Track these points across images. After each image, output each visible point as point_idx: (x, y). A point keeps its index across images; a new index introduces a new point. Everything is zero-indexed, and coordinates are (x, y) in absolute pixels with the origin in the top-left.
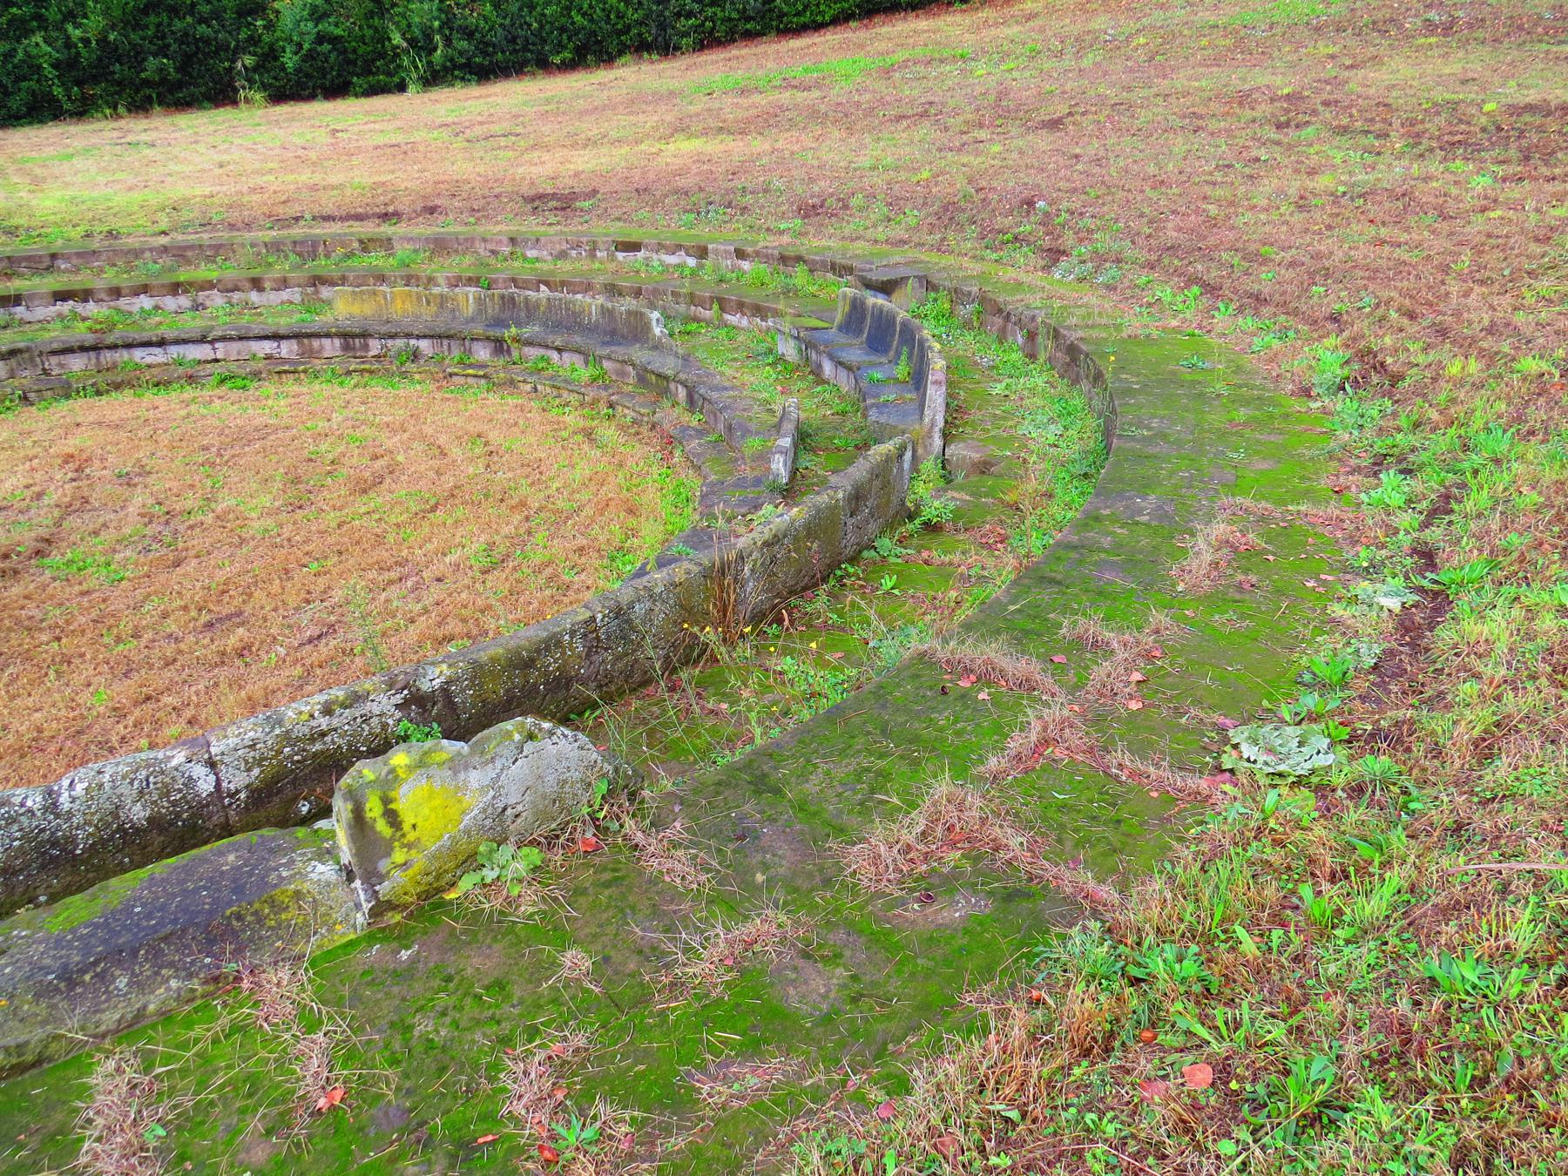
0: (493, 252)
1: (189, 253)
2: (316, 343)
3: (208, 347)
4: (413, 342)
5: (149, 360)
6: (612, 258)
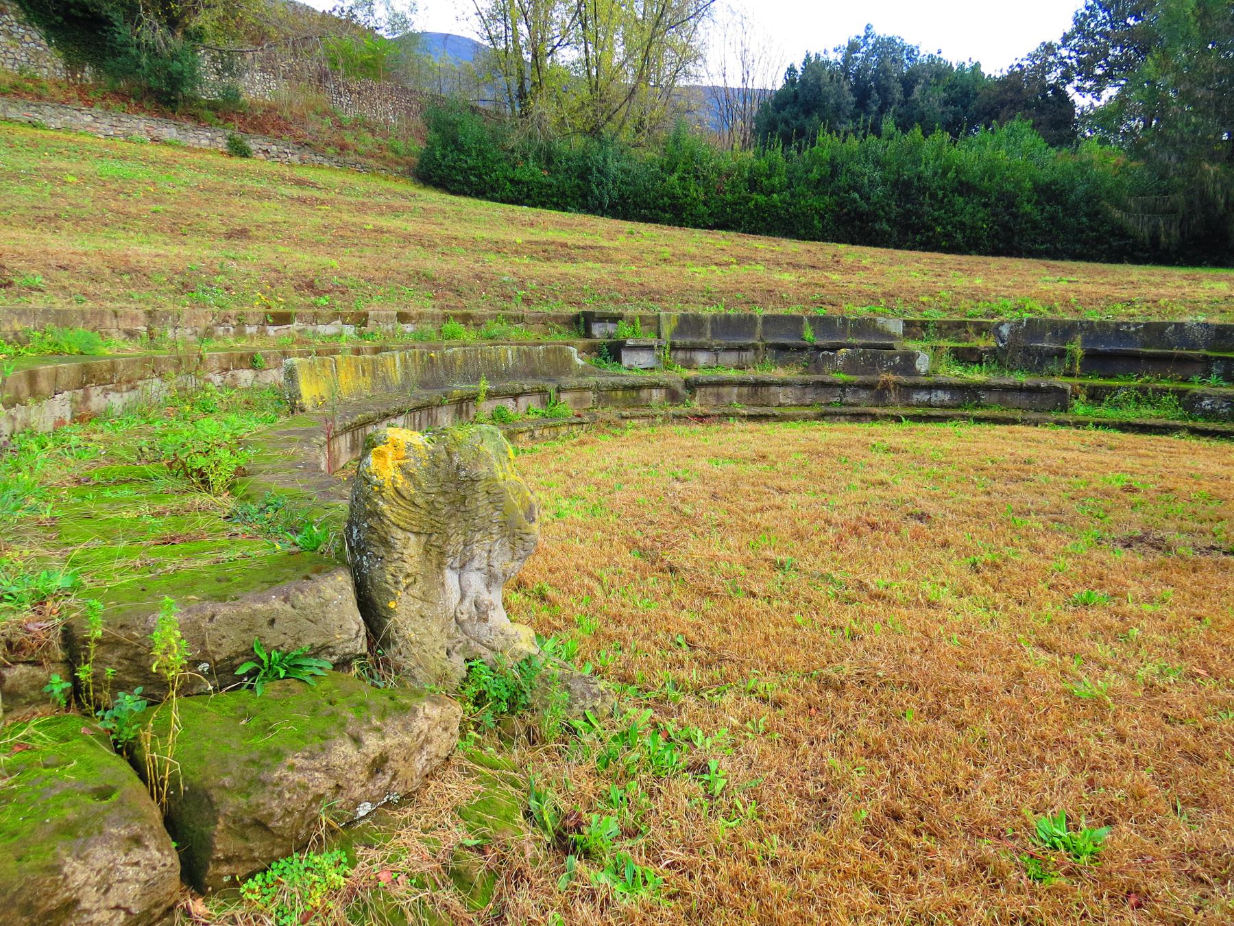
6: (262, 332)
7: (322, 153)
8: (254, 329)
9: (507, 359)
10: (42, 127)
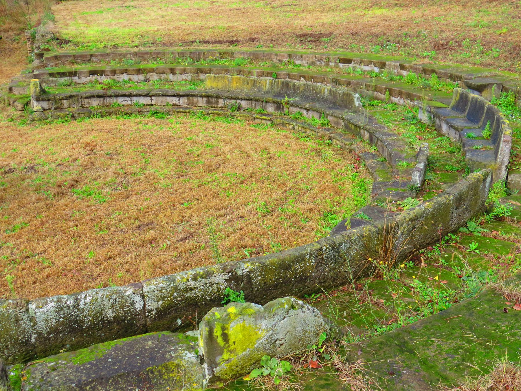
0: (280, 61)
1: (146, 56)
2: (195, 99)
3: (149, 98)
4: (239, 101)
5: (124, 103)
6: (337, 66)
9: (324, 93)
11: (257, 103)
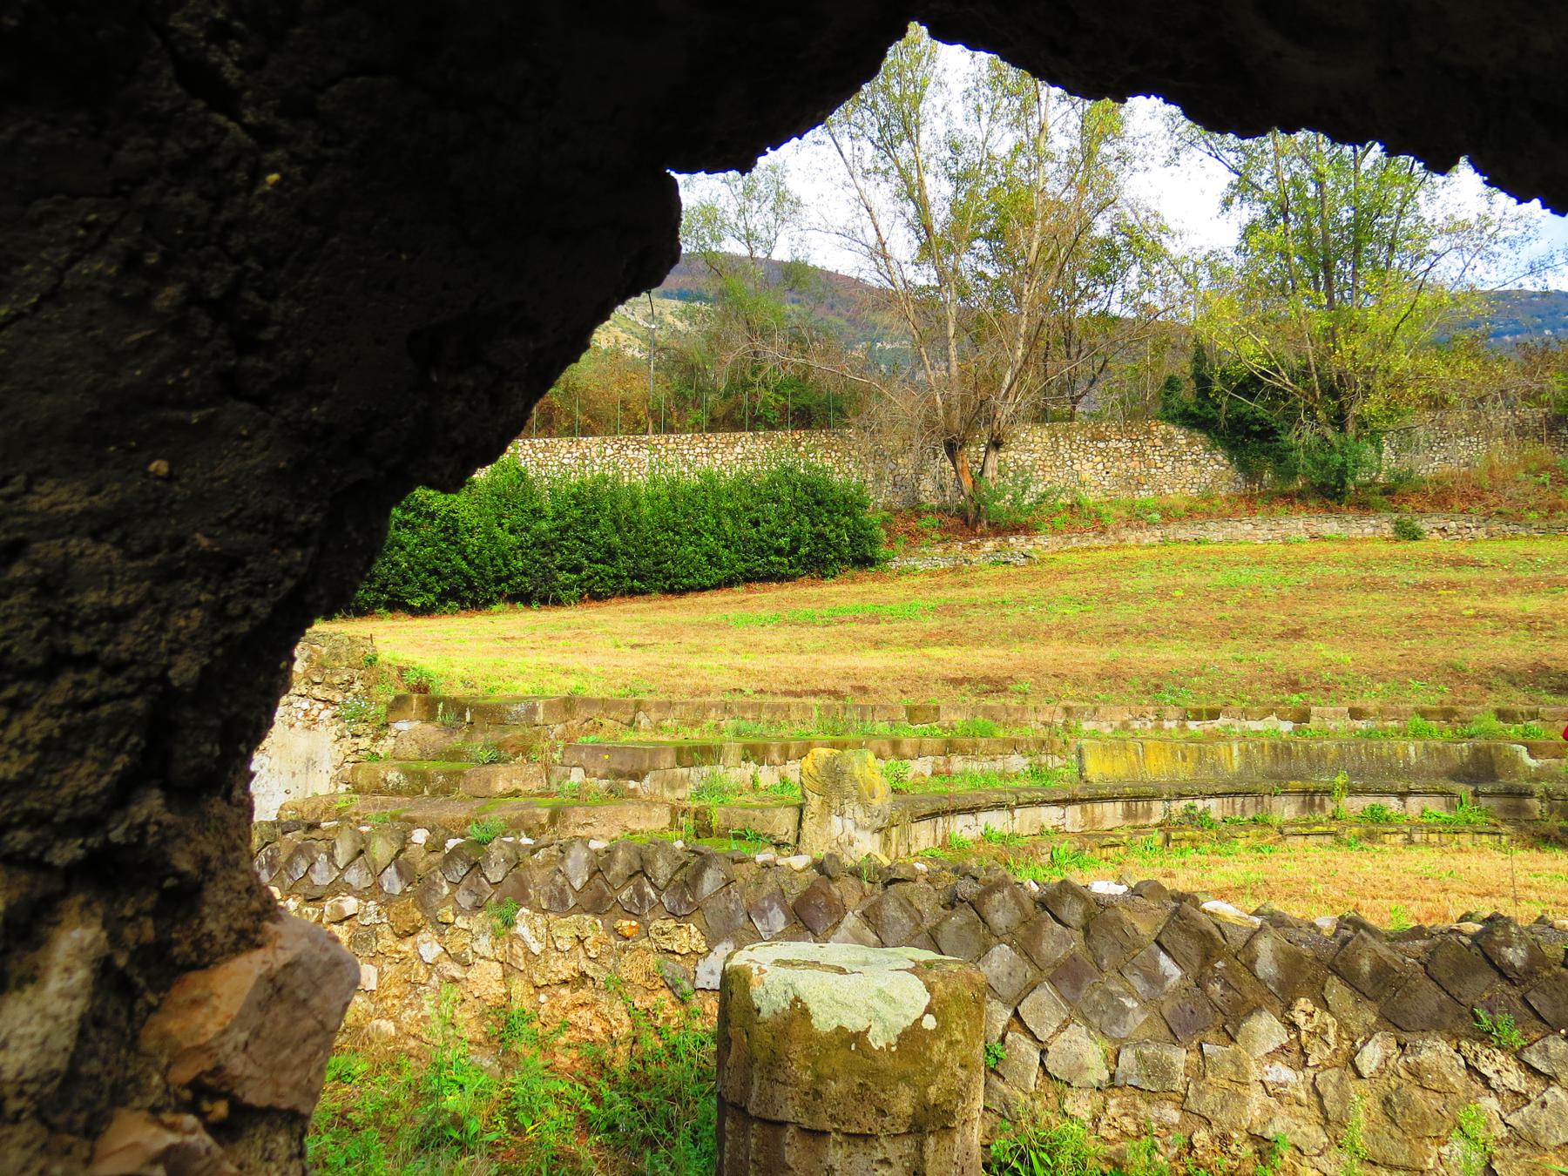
6: (1182, 728)
7: (1518, 519)
8: (1173, 724)
9: (1408, 755)
10: (1205, 542)
11: (1248, 800)
